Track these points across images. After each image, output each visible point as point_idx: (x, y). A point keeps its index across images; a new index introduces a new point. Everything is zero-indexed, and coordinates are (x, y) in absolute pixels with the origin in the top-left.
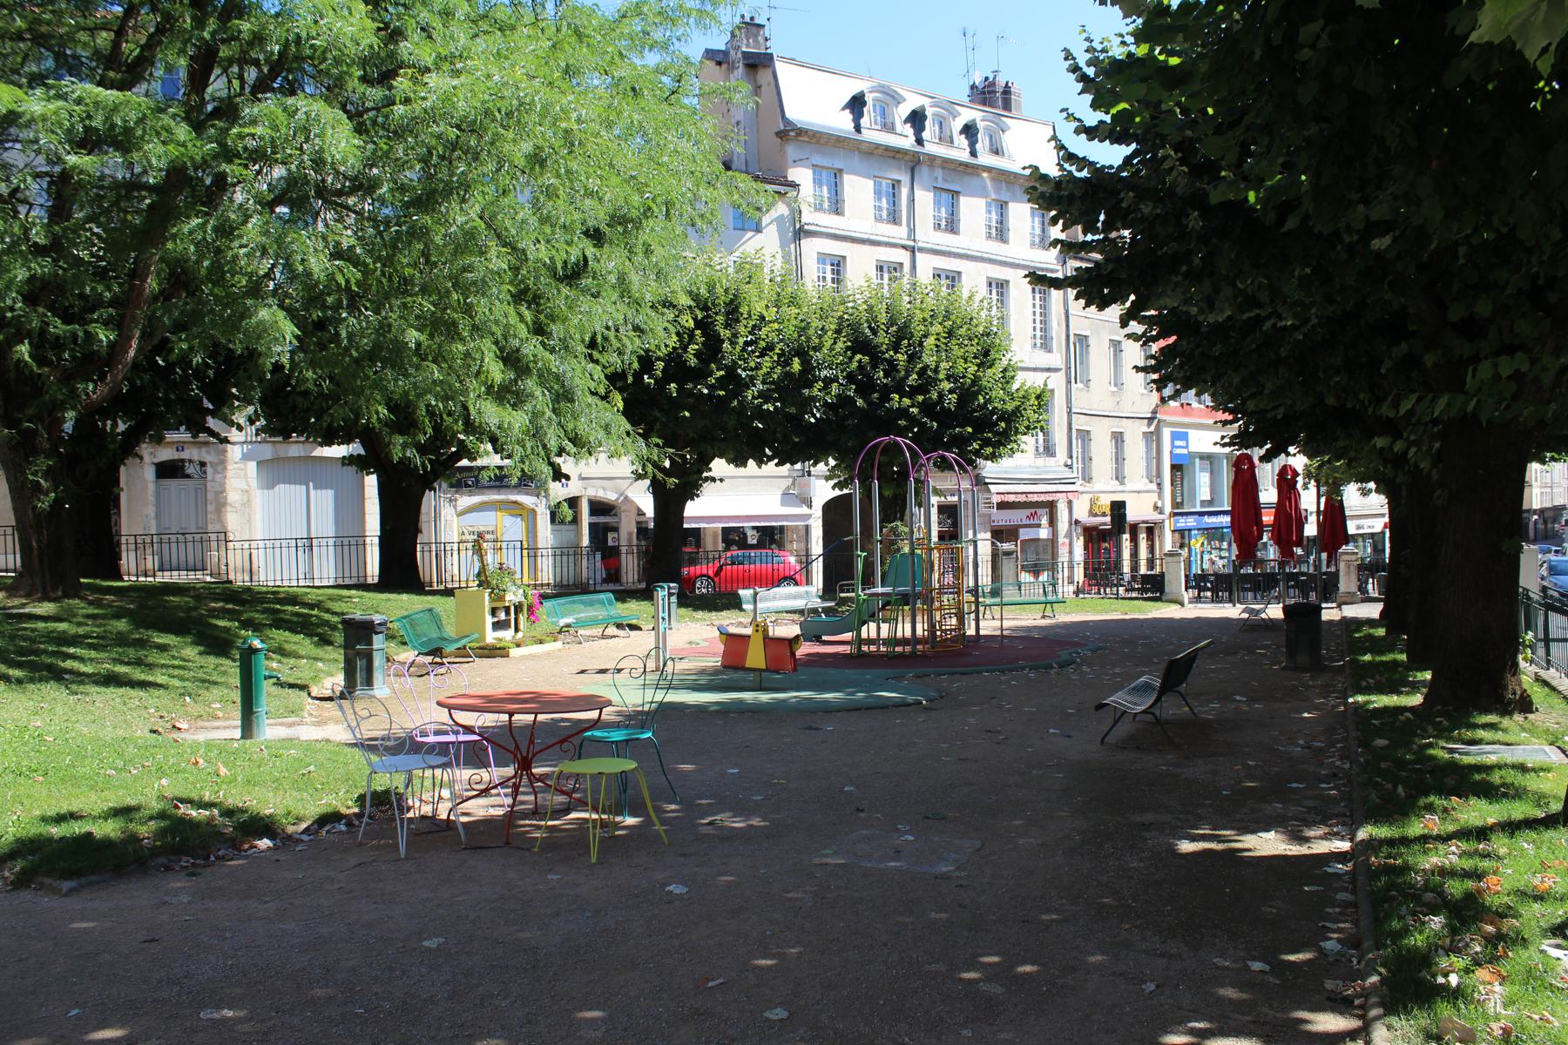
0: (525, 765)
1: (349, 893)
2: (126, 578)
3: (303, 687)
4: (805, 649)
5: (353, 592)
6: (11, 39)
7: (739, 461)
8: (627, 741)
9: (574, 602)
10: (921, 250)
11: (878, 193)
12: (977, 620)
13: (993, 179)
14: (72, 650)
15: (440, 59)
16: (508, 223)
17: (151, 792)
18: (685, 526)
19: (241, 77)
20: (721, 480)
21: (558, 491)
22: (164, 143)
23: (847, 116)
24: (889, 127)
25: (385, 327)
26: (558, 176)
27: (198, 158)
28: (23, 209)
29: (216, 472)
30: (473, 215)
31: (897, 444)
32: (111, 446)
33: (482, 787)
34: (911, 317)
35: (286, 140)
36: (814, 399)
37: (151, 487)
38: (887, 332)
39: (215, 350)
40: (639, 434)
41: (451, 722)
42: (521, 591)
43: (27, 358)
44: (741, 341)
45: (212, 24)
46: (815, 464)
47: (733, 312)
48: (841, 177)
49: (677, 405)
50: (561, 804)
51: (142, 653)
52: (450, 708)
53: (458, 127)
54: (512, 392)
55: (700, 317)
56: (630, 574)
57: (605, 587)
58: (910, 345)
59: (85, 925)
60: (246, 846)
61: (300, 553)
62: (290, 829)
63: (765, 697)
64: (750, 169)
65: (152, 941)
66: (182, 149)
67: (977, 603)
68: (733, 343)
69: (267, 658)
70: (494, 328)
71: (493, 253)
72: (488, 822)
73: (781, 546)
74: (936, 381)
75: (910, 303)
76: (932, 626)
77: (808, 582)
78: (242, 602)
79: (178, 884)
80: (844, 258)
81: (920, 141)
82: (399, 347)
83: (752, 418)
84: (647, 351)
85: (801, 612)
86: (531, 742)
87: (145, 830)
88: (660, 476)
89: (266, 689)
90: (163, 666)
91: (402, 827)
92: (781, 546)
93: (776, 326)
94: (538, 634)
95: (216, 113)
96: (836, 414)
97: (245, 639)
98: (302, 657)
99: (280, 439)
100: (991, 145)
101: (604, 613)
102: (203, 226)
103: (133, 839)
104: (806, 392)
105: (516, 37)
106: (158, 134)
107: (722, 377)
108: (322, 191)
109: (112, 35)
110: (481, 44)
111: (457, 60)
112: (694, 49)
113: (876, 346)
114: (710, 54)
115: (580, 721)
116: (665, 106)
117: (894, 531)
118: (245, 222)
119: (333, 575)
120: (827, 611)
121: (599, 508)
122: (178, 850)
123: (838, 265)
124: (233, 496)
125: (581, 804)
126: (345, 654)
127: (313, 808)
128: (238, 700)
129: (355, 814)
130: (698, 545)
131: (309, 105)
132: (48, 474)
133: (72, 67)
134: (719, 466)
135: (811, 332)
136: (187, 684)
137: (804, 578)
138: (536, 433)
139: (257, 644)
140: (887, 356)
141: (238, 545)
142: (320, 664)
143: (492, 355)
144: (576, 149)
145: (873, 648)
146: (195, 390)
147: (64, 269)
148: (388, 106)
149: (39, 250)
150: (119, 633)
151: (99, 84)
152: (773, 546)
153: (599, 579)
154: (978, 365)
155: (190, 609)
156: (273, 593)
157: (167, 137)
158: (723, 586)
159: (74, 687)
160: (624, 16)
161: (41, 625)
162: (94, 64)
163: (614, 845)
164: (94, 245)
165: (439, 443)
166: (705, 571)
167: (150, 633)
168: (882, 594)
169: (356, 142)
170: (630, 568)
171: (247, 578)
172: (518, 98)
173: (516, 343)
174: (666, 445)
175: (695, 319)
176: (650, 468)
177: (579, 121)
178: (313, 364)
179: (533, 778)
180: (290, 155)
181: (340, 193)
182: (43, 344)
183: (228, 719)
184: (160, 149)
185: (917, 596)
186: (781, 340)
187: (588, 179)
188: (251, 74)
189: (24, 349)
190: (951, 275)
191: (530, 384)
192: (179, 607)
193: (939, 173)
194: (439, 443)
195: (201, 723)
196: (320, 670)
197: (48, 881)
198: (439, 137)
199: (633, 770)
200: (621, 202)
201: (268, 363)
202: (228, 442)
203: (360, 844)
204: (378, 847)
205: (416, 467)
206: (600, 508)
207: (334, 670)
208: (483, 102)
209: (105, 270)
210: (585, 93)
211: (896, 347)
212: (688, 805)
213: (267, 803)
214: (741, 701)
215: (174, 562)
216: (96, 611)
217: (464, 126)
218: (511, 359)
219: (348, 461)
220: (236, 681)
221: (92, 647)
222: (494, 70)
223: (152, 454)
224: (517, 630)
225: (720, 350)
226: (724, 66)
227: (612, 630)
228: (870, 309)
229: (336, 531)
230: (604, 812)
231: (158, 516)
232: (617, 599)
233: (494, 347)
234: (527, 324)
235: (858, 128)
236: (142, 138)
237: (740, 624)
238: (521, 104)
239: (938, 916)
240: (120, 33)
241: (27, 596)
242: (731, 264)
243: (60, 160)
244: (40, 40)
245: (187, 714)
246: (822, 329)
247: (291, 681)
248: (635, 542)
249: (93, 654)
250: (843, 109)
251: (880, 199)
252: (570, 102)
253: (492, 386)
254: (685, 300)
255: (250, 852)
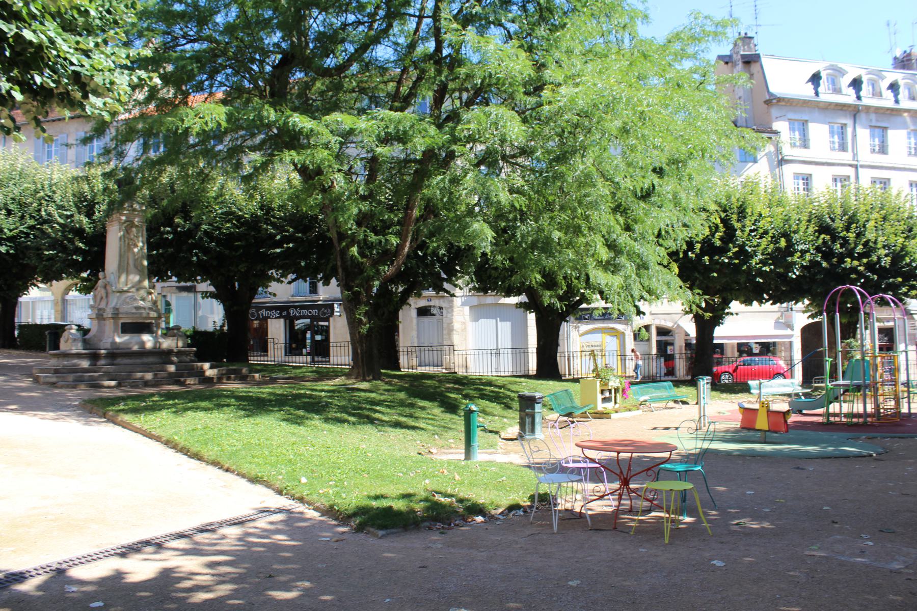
0: (625, 482)
1: (527, 550)
2: (402, 370)
3: (497, 433)
4: (793, 418)
5: (522, 380)
6: (350, 92)
7: (748, 302)
8: (686, 471)
9: (649, 387)
10: (862, 166)
11: (832, 133)
12: (909, 403)
13: (911, 117)
14: (378, 408)
15: (567, 78)
16: (608, 167)
17: (421, 486)
18: (715, 342)
19: (460, 98)
20: (737, 314)
21: (638, 322)
22: (423, 137)
23: (810, 86)
24: (837, 91)
25: (540, 230)
26: (637, 138)
27: (440, 144)
28: (354, 177)
29: (448, 312)
30: (588, 164)
31: (851, 291)
32: (395, 299)
33: (601, 494)
34: (857, 209)
35: (486, 130)
36: (795, 263)
37: (415, 321)
38: (841, 220)
39: (450, 247)
40: (687, 287)
41: (583, 456)
42: (618, 380)
43: (356, 254)
44: (747, 229)
45: (445, 72)
46: (796, 304)
47: (742, 213)
48: (807, 125)
49: (709, 269)
50: (646, 507)
51: (412, 411)
52: (583, 447)
53: (578, 115)
54: (611, 265)
55: (723, 216)
56: (682, 370)
57: (667, 378)
58: (857, 227)
59: (390, 555)
60: (470, 520)
61: (493, 357)
62: (493, 512)
63: (768, 448)
64: (749, 125)
65: (424, 567)
66: (432, 140)
67: (909, 392)
68: (742, 231)
69: (479, 416)
70: (602, 228)
71: (600, 185)
72: (603, 515)
73: (774, 354)
74: (875, 250)
75: (856, 200)
76: (877, 407)
77: (792, 376)
78: (463, 384)
79: (435, 538)
80: (811, 175)
81: (859, 98)
82: (548, 241)
83: (755, 276)
84: (691, 238)
85: (789, 395)
86: (629, 469)
87: (419, 507)
88: (700, 312)
89: (478, 434)
90: (423, 418)
91: (555, 515)
92: (774, 354)
93: (769, 219)
94: (628, 406)
95: (448, 119)
96: (809, 272)
97: (467, 405)
98: (495, 415)
99: (482, 294)
100: (910, 94)
101: (667, 394)
102: (443, 179)
103: (412, 511)
104: (789, 259)
105: (608, 60)
106: (420, 132)
107: (737, 251)
108: (504, 158)
109: (395, 84)
110: (590, 66)
111: (577, 77)
112: (712, 57)
113: (834, 229)
114: (720, 57)
115: (655, 458)
116: (697, 93)
117: (849, 345)
118: (465, 176)
119: (511, 369)
120: (805, 395)
121: (662, 331)
122: (436, 519)
123: (807, 179)
124: (457, 326)
125: (659, 508)
126: (520, 415)
127: (505, 501)
128: (463, 438)
129: (528, 506)
130: (722, 353)
131: (496, 110)
132: (366, 314)
133: (375, 101)
134: (735, 306)
135: (791, 222)
136: (435, 428)
137: (789, 374)
138: (627, 288)
139: (474, 408)
140: (841, 235)
141: (460, 353)
142: (505, 420)
143: (601, 244)
144: (647, 122)
145: (837, 419)
146: (437, 268)
147: (375, 207)
148: (540, 106)
149: (363, 198)
150: (401, 399)
151: (391, 109)
152: (769, 354)
153: (663, 374)
154: (905, 238)
155: (436, 387)
156: (479, 379)
157: (424, 133)
158: (738, 378)
159: (380, 428)
160: (670, 42)
161: (363, 394)
162: (387, 99)
163: (678, 533)
164: (387, 193)
165: (569, 295)
166: (727, 370)
167: (416, 400)
168: (843, 385)
169: (523, 128)
170: (681, 367)
171: (464, 371)
172: (613, 96)
173: (615, 236)
174: (704, 294)
175: (720, 217)
176: (694, 307)
177: (648, 105)
178: (501, 252)
179: (630, 491)
180: (488, 138)
181: (513, 156)
182: (365, 246)
183: (457, 448)
184: (422, 141)
185: (866, 386)
186: (773, 228)
187: (654, 139)
188: (465, 95)
189: (354, 250)
190: (883, 181)
191: (623, 260)
192: (430, 386)
193: (873, 116)
194: (569, 295)
195: (443, 450)
196: (506, 423)
197: (372, 530)
198: (567, 122)
199: (690, 489)
200: (674, 151)
201: (479, 253)
202: (455, 296)
203: (531, 523)
204: (541, 525)
205: (558, 309)
206: (662, 331)
207: (513, 423)
208: (592, 100)
209: (392, 206)
210: (651, 89)
211: (848, 229)
212: (723, 512)
213: (481, 497)
214: (753, 450)
215: (427, 362)
216: (389, 388)
217: (582, 114)
218: (612, 246)
219: (520, 305)
220: (463, 429)
221: (388, 406)
222: (597, 81)
223: (415, 303)
224: (616, 403)
225: (734, 236)
226: (730, 64)
227: (671, 404)
228: (830, 206)
229: (512, 345)
230: (673, 514)
231: (418, 337)
232: (674, 386)
233: (602, 239)
234: (620, 225)
235: (817, 94)
236: (412, 135)
237: (749, 402)
238: (615, 99)
239: (894, 598)
240: (399, 82)
241: (356, 378)
242: (739, 183)
243: (372, 150)
244: (362, 91)
245: (436, 445)
246: (799, 220)
247: (490, 429)
248: (684, 351)
249: (388, 410)
250: (807, 82)
251: (833, 137)
252: (642, 95)
253: (602, 262)
254: (713, 207)
255: (472, 523)
